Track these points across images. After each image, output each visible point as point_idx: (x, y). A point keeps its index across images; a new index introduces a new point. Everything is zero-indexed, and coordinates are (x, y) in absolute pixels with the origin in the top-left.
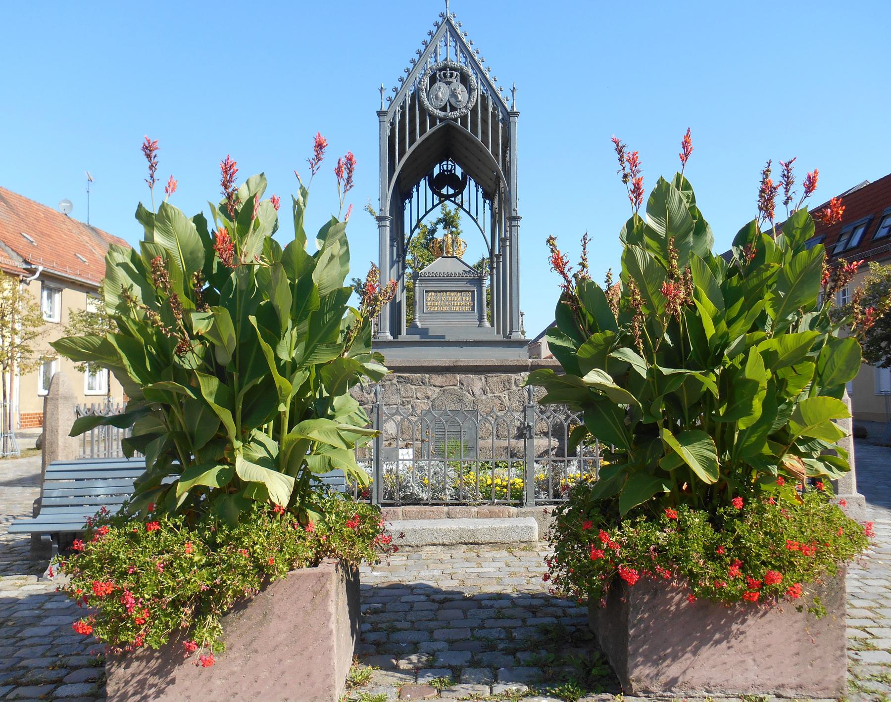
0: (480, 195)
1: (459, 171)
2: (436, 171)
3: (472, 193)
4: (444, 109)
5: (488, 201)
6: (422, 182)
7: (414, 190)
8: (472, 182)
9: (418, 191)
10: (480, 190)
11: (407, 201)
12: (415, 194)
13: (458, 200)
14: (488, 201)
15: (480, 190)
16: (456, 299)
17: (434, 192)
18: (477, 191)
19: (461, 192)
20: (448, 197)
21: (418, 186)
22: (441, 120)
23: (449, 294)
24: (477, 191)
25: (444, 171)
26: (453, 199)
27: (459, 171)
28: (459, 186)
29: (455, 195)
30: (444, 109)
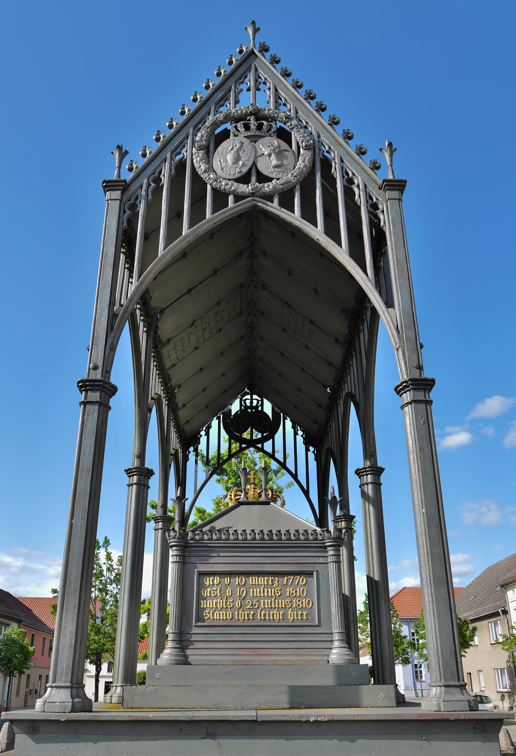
0: (300, 439)
1: (268, 408)
2: (235, 407)
3: (288, 437)
4: (244, 179)
5: (311, 449)
6: (215, 423)
7: (203, 433)
8: (289, 423)
9: (207, 434)
10: (300, 433)
11: (191, 449)
12: (203, 440)
13: (268, 446)
14: (311, 449)
15: (300, 433)
16: (270, 592)
17: (232, 437)
18: (296, 434)
19: (271, 436)
20: (252, 443)
21: (209, 427)
22: (238, 198)
23: (252, 580)
24: (296, 434)
25: (246, 407)
26: (260, 446)
27: (268, 408)
28: (269, 428)
29: (263, 440)
30: (244, 179)
